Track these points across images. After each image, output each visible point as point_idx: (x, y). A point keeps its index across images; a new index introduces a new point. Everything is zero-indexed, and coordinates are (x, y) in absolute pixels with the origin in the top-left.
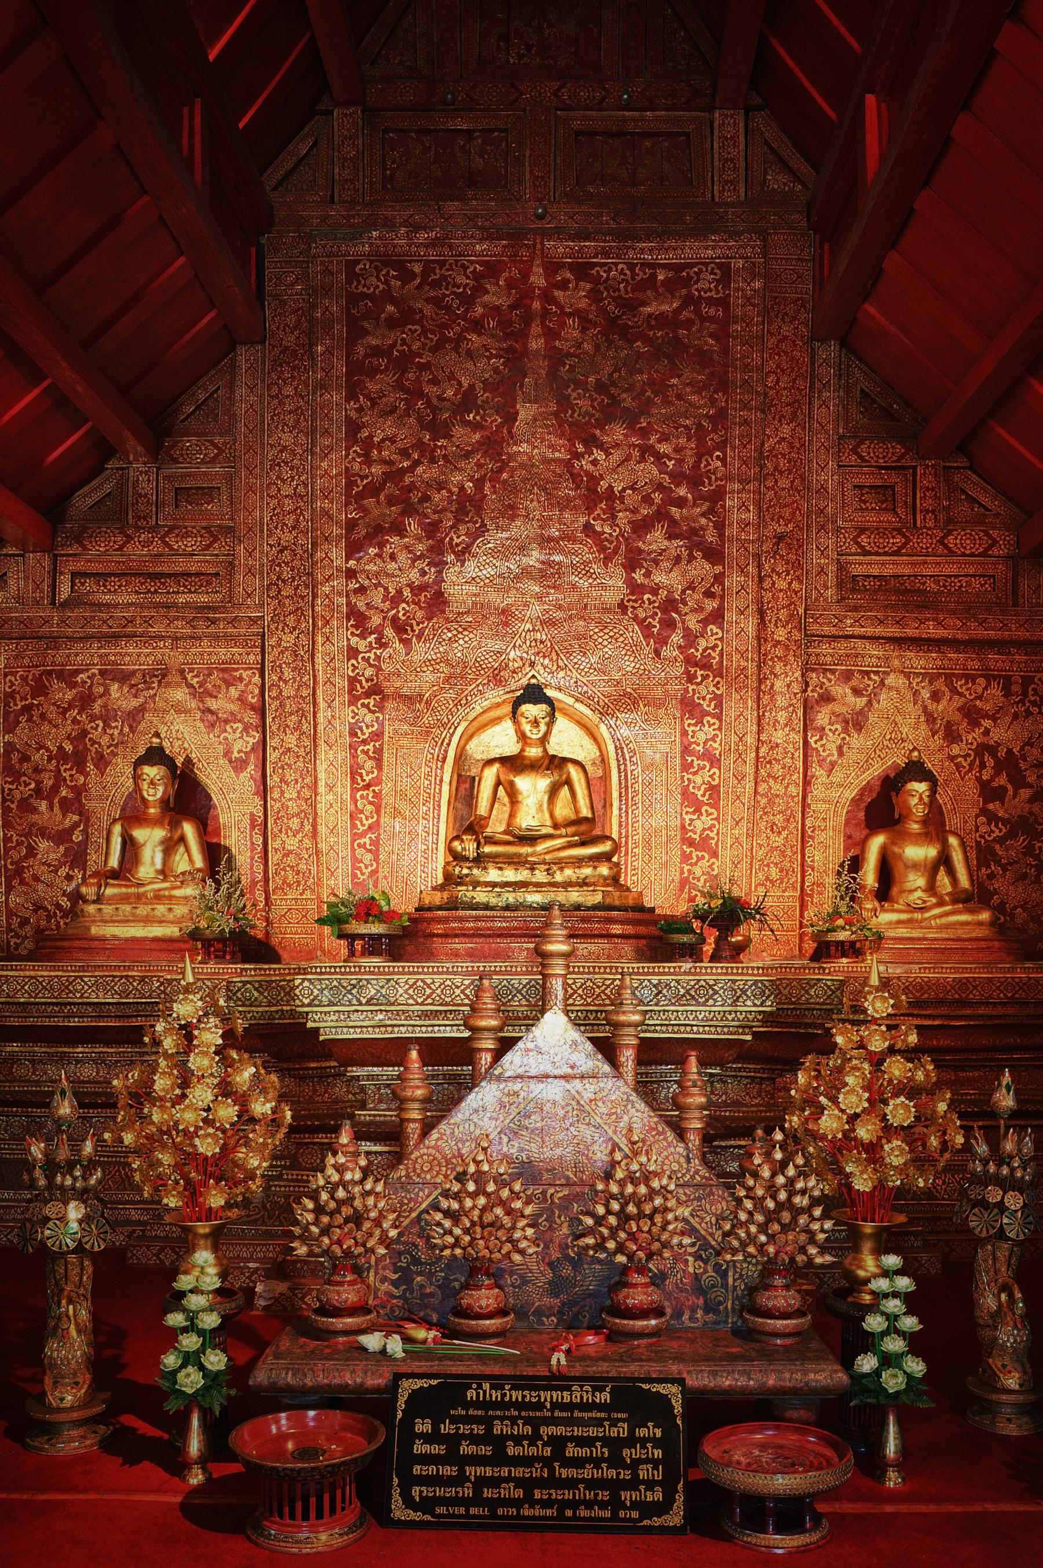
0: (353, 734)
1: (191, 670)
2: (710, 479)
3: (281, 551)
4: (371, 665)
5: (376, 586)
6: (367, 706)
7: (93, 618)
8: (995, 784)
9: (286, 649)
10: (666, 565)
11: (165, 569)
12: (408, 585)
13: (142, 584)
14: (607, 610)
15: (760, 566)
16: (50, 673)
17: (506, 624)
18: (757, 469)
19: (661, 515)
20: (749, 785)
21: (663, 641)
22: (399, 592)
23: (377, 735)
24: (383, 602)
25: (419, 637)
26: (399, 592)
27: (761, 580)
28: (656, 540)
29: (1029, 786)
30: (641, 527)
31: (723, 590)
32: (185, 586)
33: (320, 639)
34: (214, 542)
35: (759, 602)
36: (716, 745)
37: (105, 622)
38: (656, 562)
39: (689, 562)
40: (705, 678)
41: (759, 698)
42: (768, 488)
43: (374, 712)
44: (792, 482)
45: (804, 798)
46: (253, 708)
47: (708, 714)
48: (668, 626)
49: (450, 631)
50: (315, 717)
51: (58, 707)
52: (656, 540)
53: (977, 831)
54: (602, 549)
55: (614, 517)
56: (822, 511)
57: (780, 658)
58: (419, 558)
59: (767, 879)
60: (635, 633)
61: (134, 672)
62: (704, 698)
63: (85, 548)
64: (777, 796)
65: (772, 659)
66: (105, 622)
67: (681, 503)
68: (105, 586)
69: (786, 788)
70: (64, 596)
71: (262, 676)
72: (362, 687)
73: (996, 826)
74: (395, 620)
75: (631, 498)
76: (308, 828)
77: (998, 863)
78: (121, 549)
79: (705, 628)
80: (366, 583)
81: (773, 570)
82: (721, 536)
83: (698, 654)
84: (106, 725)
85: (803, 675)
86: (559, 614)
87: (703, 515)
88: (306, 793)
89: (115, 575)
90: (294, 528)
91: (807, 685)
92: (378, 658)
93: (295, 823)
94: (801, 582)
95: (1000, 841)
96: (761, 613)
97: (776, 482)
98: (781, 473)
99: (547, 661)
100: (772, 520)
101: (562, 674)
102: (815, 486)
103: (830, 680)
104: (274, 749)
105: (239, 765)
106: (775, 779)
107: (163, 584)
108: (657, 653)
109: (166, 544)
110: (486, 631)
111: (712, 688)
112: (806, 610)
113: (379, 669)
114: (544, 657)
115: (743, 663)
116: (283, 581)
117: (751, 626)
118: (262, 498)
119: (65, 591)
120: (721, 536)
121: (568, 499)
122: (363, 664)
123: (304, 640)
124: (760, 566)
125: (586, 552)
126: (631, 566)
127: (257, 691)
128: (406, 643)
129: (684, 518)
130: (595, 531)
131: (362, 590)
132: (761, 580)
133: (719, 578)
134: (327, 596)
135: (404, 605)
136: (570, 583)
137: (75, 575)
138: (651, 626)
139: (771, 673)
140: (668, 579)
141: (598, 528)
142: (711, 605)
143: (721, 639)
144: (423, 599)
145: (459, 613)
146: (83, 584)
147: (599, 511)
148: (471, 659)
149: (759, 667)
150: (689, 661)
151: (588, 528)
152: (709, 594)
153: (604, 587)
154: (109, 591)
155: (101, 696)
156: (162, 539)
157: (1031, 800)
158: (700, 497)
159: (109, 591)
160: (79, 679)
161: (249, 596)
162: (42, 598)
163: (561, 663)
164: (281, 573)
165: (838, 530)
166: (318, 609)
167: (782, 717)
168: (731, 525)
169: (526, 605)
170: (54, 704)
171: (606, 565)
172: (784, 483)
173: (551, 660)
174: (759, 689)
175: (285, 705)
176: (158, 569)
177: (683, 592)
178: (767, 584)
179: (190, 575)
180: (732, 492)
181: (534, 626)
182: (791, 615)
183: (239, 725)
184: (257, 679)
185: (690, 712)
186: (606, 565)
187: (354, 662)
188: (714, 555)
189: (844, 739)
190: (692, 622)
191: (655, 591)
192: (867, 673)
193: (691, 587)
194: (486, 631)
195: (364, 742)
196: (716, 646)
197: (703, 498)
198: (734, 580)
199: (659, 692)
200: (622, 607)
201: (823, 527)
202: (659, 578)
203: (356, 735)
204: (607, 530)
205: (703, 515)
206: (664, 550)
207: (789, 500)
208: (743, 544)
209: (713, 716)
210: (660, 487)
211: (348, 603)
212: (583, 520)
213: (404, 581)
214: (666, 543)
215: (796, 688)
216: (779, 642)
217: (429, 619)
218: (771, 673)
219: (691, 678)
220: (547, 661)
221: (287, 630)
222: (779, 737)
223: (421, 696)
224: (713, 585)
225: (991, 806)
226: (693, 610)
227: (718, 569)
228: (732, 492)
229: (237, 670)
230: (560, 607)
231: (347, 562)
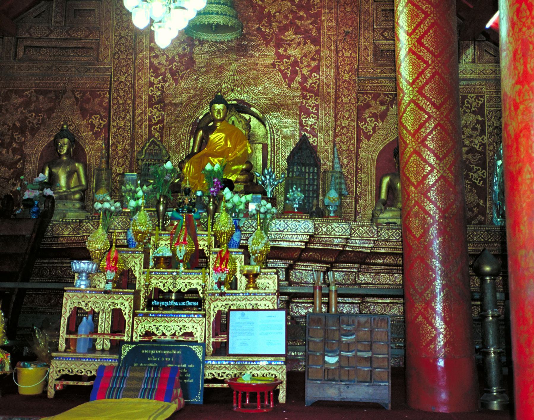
0: (150, 121)
1: (77, 91)
2: (314, 8)
3: (121, 38)
4: (159, 90)
5: (163, 55)
6: (157, 108)
7: (33, 67)
9: (121, 82)
10: (294, 46)
11: (68, 46)
12: (177, 54)
13: (57, 52)
14: (266, 66)
15: (337, 47)
16: (11, 91)
17: (221, 72)
18: (336, 3)
19: (292, 24)
20: (330, 144)
21: (292, 80)
22: (173, 57)
23: (161, 121)
24: (166, 61)
25: (182, 78)
26: (173, 57)
27: (337, 52)
28: (290, 35)
30: (283, 29)
31: (320, 57)
32: (77, 53)
33: (137, 78)
34: (91, 34)
35: (336, 62)
36: (316, 127)
37: (38, 68)
38: (290, 45)
39: (304, 44)
40: (311, 97)
41: (336, 106)
42: (341, 12)
43: (160, 111)
44: (352, 9)
45: (357, 152)
46: (105, 108)
47: (312, 113)
48: (294, 73)
49: (195, 75)
50: (133, 113)
51: (15, 106)
52: (290, 35)
54: (265, 39)
55: (271, 25)
56: (366, 21)
57: (346, 88)
58: (183, 42)
60: (280, 76)
61: (52, 90)
62: (310, 106)
63: (31, 35)
64: (344, 150)
65: (342, 88)
66: (38, 68)
67: (301, 18)
68: (40, 53)
69: (348, 147)
70: (20, 57)
71: (110, 94)
72: (155, 100)
74: (171, 69)
75: (279, 17)
76: (127, 163)
78: (48, 35)
79: (311, 74)
80: (159, 53)
81: (343, 48)
82: (319, 33)
83: (308, 86)
84: (37, 115)
85: (356, 95)
86: (245, 68)
87: (311, 24)
88: (127, 147)
89: (45, 47)
90: (127, 28)
91: (358, 99)
92: (162, 87)
93: (121, 161)
94: (356, 53)
96: (337, 68)
97: (345, 9)
98: (347, 5)
99: (239, 89)
100: (343, 25)
101: (245, 95)
102: (363, 10)
103: (369, 98)
104: (114, 127)
105: (97, 135)
106: (343, 143)
107: (67, 52)
108: (289, 85)
109: (69, 34)
110: (212, 75)
111: (314, 102)
112: (358, 66)
113: (163, 92)
114: (238, 87)
115: (329, 90)
116: (121, 52)
117: (332, 73)
118: (113, 15)
119: (21, 53)
120: (319, 33)
121: (250, 17)
122: (156, 89)
123: (130, 78)
124: (337, 47)
125: (258, 40)
126: (278, 45)
127: (107, 101)
128: (176, 80)
129: (303, 25)
130: (262, 31)
131: (156, 56)
132: (337, 52)
133: (318, 52)
134: (141, 59)
135: (175, 63)
136: (250, 54)
137: (26, 47)
138: (286, 73)
139: (342, 94)
140: (295, 52)
141: (263, 30)
142: (314, 64)
143: (319, 79)
144: (184, 61)
145: (200, 67)
146: (29, 51)
147: (264, 22)
148: (205, 88)
149: (336, 91)
150: (304, 89)
151: (259, 29)
152: (313, 59)
153: (266, 56)
154: (41, 55)
155: (35, 102)
156: (67, 32)
158: (310, 16)
159: (41, 55)
160: (25, 94)
161: (105, 58)
162: (10, 57)
163: (245, 90)
164: (121, 48)
165: (374, 30)
166: (136, 64)
167: (347, 114)
168: (324, 28)
169: (230, 64)
170: (13, 105)
171: (267, 47)
172: (349, 9)
173: (241, 88)
174: (336, 102)
175: (120, 107)
176: (65, 46)
177: (302, 58)
178: (340, 54)
179: (79, 48)
180: (324, 13)
181: (234, 73)
182: (351, 68)
183: (98, 116)
184: (107, 95)
185: (303, 112)
186: (267, 47)
187: (152, 88)
188: (316, 41)
189: (376, 124)
190: (305, 71)
191: (288, 58)
192: (387, 94)
193: (305, 56)
194: (212, 75)
195: (156, 124)
196: (317, 82)
197: (312, 16)
198: (325, 53)
199: (290, 102)
200: (274, 65)
201: (367, 28)
202: (290, 52)
203: (151, 121)
204: (267, 30)
205: (311, 24)
206: (293, 39)
207: (351, 17)
208: (329, 37)
209: (314, 114)
210: (292, 11)
211: (150, 62)
212: (257, 26)
213: (176, 53)
214: (294, 36)
215: (353, 101)
216: (345, 80)
217: (186, 70)
218: (342, 94)
219: (304, 97)
220: (239, 89)
221: (122, 74)
222: (345, 123)
223: (181, 104)
224: (315, 55)
226: (306, 66)
227: (317, 48)
228: (324, 13)
229: (98, 91)
230: (245, 65)
231: (150, 44)
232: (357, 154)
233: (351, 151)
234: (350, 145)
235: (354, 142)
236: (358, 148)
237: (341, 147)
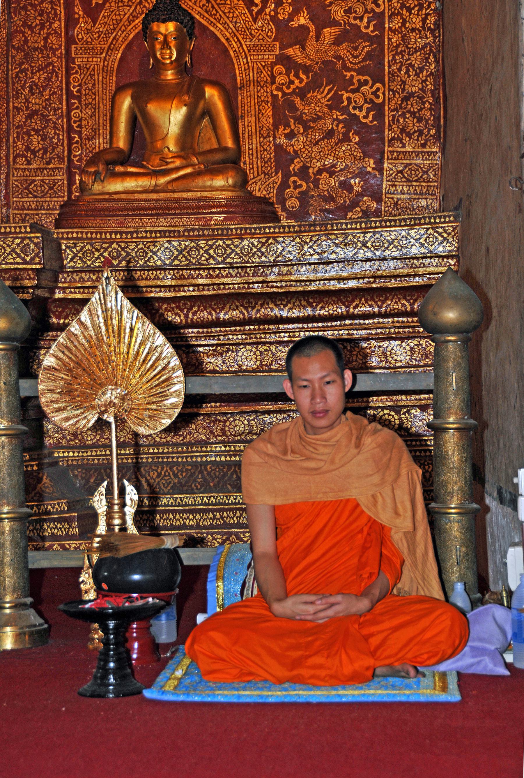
8: (294, 24)
29: (335, 23)
53: (273, 82)
59: (28, 149)
64: (35, 49)
69: (46, 39)
73: (297, 76)
77: (299, 120)
95: (302, 93)
106: (30, 28)
157: (337, 42)
225: (290, 51)
232: (69, 59)
233: (54, 51)
234: (48, 34)
235: (60, 25)
236: (70, 41)
237: (26, 41)
